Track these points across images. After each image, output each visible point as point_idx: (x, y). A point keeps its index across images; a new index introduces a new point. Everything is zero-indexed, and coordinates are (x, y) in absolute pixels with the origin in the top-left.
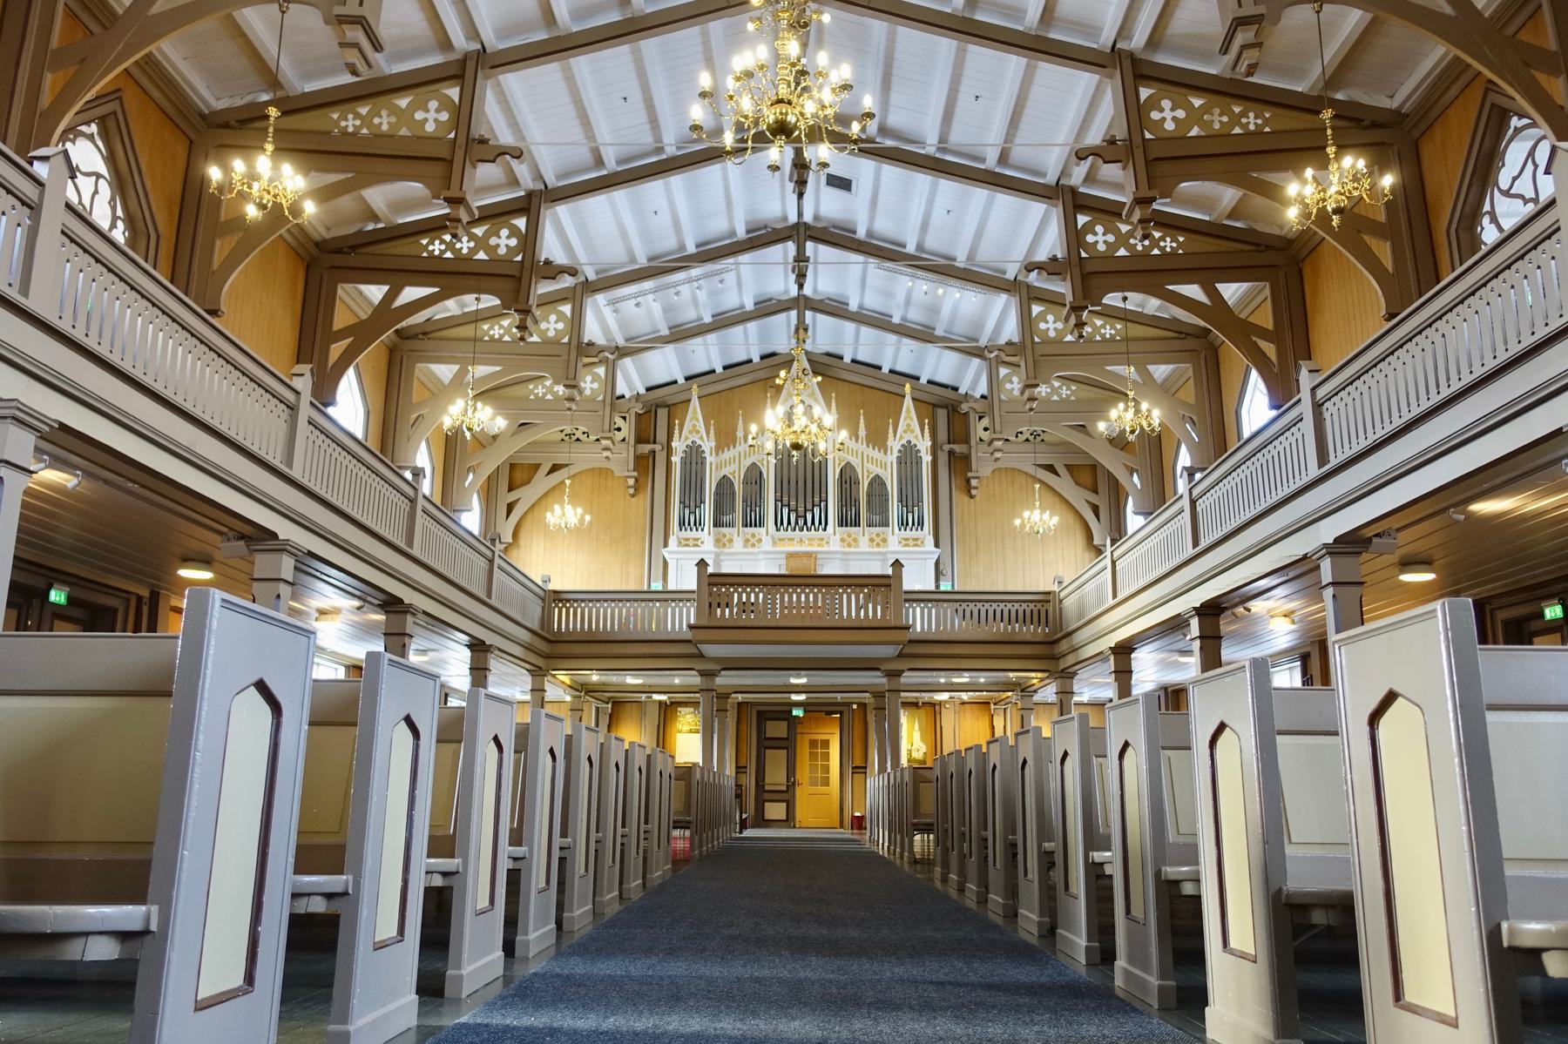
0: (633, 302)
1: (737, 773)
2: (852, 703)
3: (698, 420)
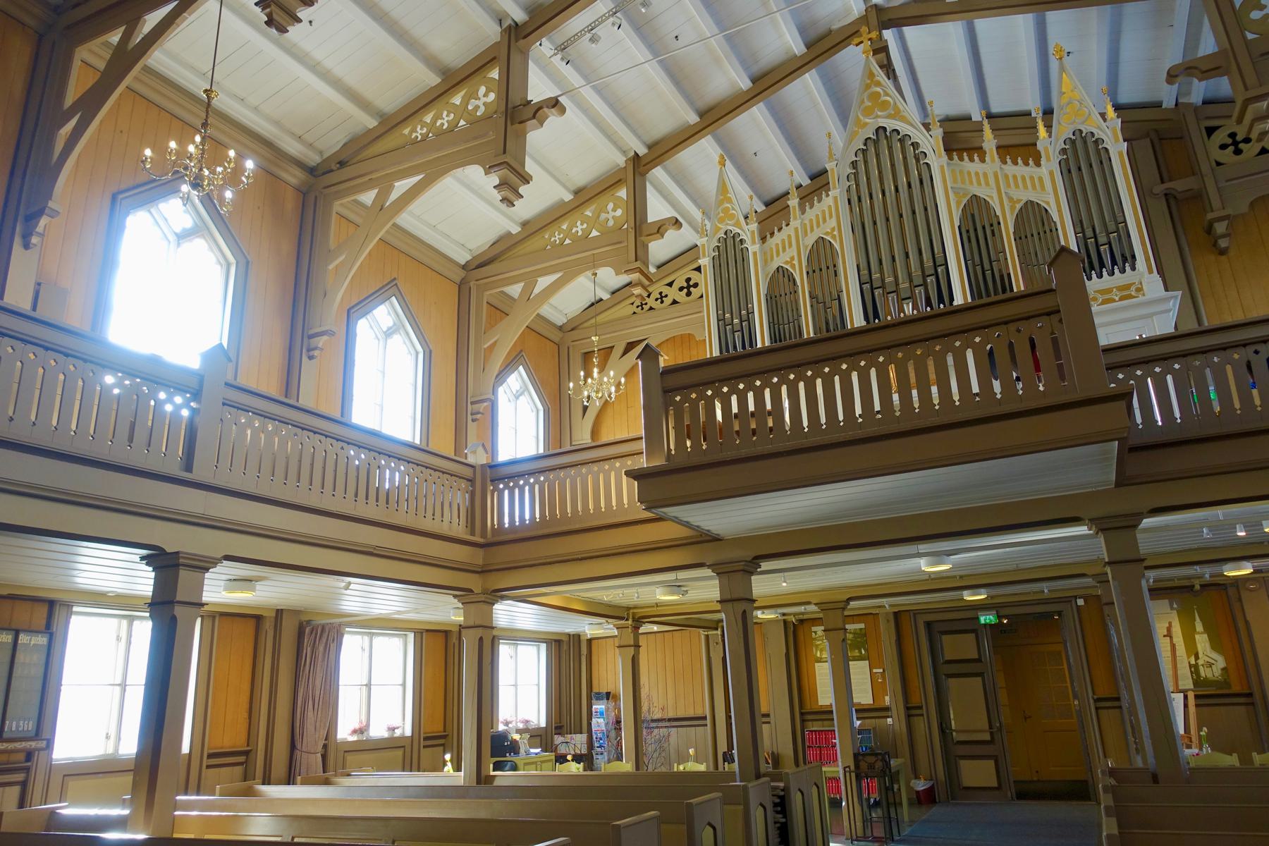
0: (588, 36)
1: (909, 716)
2: (1076, 597)
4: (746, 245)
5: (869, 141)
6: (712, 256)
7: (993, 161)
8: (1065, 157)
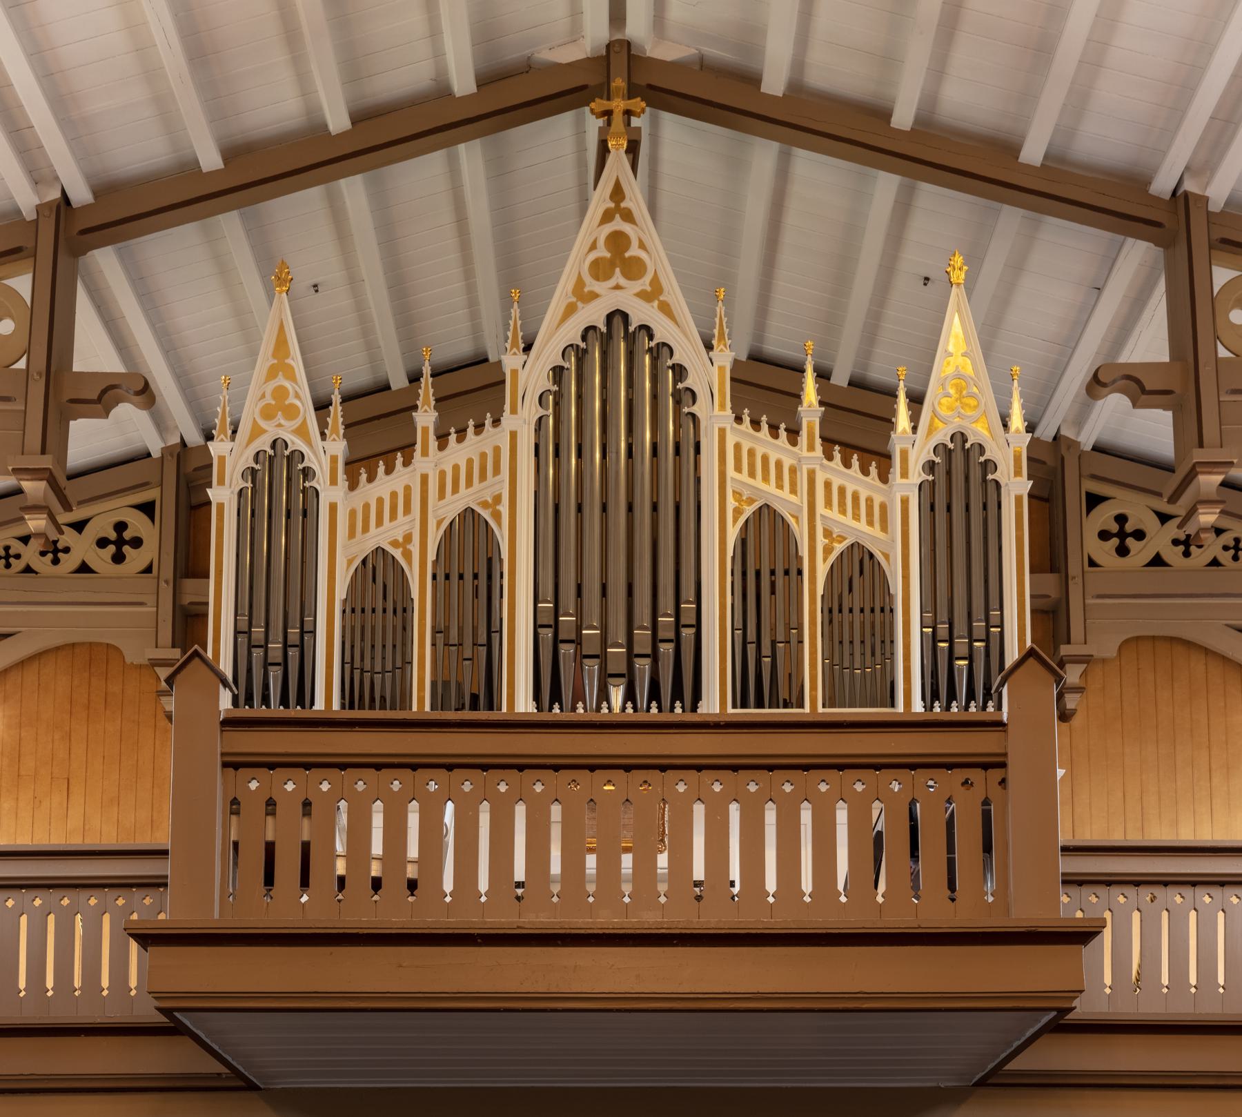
3: (292, 377)
4: (314, 484)
5: (591, 333)
6: (237, 490)
7: (811, 448)
8: (931, 478)
